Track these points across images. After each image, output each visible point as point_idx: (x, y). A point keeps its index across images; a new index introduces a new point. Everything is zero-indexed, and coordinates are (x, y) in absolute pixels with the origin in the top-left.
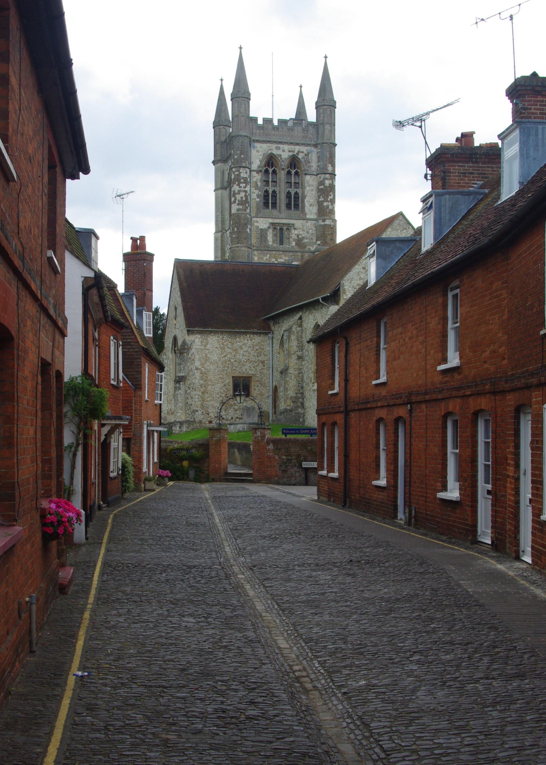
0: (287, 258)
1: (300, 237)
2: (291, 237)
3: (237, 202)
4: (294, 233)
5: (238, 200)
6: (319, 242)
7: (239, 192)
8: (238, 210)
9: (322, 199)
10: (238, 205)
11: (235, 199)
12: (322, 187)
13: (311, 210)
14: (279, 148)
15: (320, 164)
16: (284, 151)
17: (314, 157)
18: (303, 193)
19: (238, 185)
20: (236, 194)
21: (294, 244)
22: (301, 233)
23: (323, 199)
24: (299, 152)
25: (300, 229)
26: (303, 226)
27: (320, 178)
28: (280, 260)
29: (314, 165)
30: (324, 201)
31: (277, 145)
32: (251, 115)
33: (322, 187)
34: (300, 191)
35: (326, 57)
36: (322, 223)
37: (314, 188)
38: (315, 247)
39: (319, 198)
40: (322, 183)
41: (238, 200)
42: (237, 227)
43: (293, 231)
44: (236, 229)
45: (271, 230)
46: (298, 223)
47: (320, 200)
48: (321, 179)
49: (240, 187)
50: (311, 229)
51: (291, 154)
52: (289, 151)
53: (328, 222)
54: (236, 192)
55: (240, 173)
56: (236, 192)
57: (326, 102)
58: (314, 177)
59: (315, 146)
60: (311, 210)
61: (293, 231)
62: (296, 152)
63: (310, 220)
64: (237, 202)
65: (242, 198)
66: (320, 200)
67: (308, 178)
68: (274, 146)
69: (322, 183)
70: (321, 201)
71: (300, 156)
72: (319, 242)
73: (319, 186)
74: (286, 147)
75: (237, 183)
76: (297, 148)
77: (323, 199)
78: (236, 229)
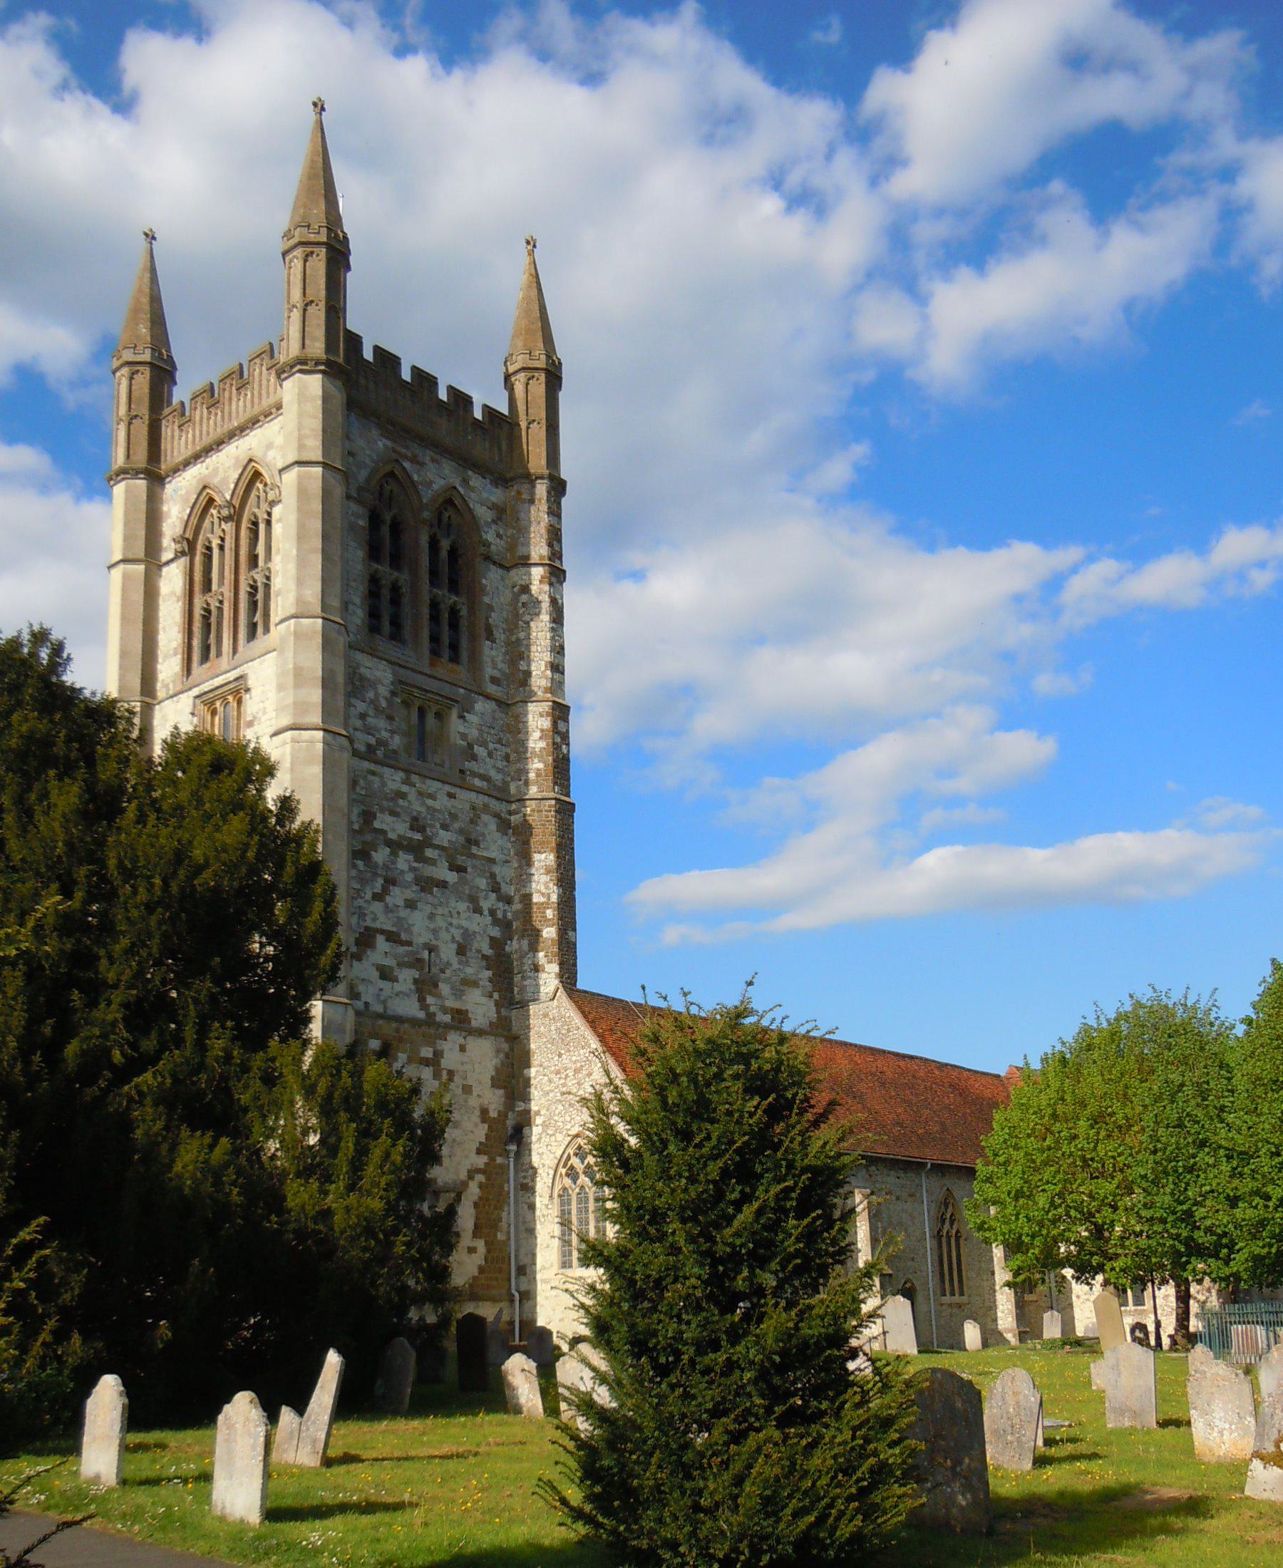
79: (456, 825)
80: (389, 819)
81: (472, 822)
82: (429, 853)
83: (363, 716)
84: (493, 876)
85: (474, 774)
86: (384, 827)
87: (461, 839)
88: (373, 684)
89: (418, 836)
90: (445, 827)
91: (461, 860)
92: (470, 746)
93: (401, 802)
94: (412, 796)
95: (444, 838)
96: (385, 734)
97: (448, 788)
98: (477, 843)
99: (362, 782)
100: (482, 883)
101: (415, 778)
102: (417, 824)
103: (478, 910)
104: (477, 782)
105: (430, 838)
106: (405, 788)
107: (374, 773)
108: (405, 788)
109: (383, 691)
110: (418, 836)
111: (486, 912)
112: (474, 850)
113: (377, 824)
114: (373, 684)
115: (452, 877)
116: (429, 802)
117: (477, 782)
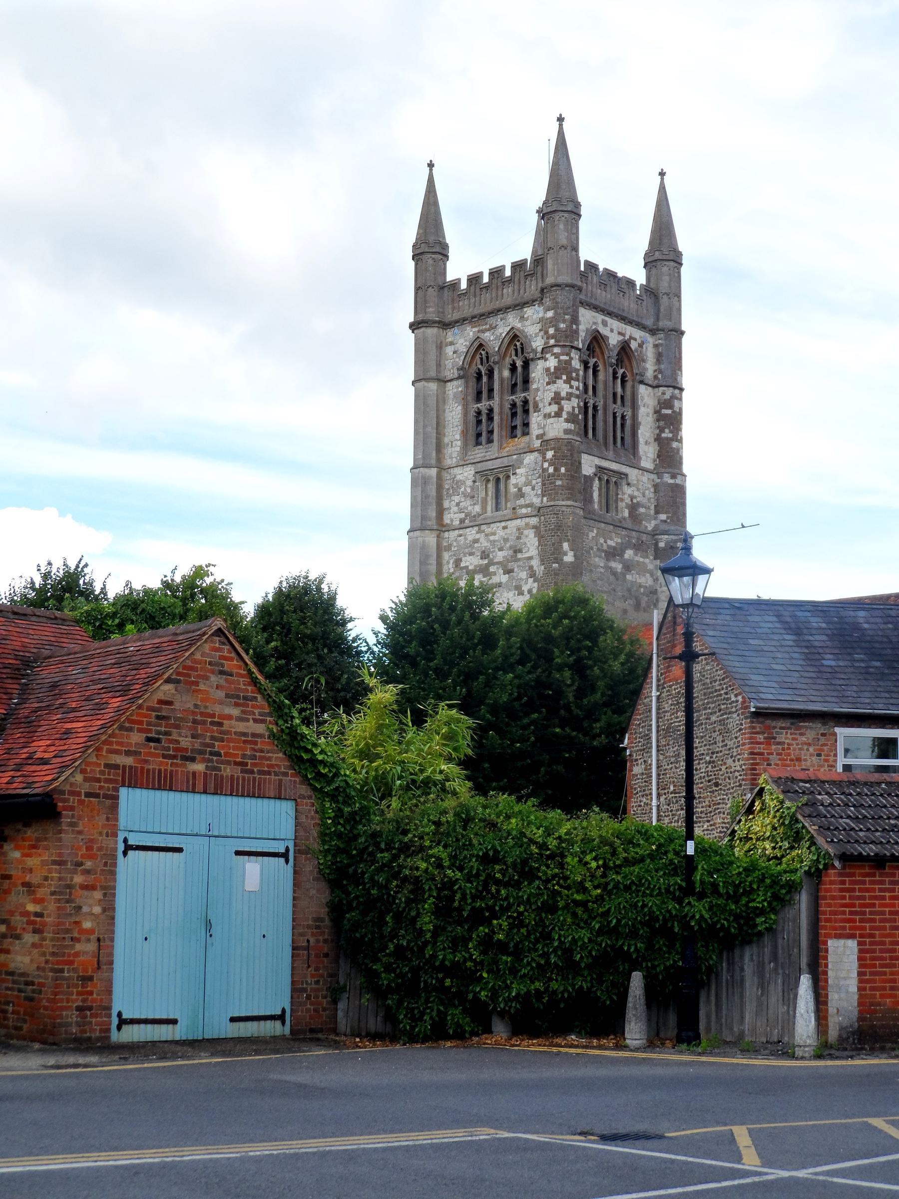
0: (619, 540)
1: (635, 501)
2: (622, 500)
3: (565, 415)
4: (627, 491)
5: (568, 413)
6: (663, 517)
7: (569, 396)
8: (567, 431)
9: (667, 434)
10: (567, 421)
11: (561, 409)
12: (669, 412)
13: (648, 452)
14: (605, 324)
15: (662, 367)
16: (612, 331)
17: (650, 353)
18: (634, 417)
19: (567, 382)
20: (563, 399)
21: (626, 513)
22: (636, 493)
23: (670, 435)
24: (631, 338)
25: (634, 485)
26: (638, 481)
27: (664, 393)
28: (610, 543)
29: (650, 368)
30: (672, 439)
31: (603, 317)
32: (586, 253)
33: (669, 412)
34: (629, 414)
35: (662, 174)
36: (671, 481)
37: (650, 411)
38: (653, 523)
39: (662, 430)
40: (668, 404)
41: (568, 413)
42: (565, 465)
43: (625, 488)
44: (563, 470)
45: (596, 482)
46: (633, 473)
47: (663, 435)
48: (667, 396)
49: (571, 387)
50: (648, 489)
51: (621, 338)
52: (620, 333)
53: (678, 481)
54: (563, 394)
55: (571, 359)
56: (563, 394)
57: (663, 252)
58: (650, 389)
59: (653, 332)
60: (648, 452)
61: (625, 488)
62: (627, 337)
63: (647, 471)
64: (565, 415)
65: (573, 408)
66: (663, 435)
67: (642, 389)
68: (600, 317)
69: (668, 404)
70: (667, 438)
71: (634, 345)
72: (663, 517)
73: (661, 408)
74: (614, 324)
75: (564, 377)
76: (630, 331)
77: (670, 435)
78: (563, 470)
79: (508, 545)
80: (468, 558)
81: (519, 538)
82: (492, 569)
83: (458, 504)
84: (531, 568)
85: (521, 507)
86: (468, 564)
87: (511, 552)
88: (463, 483)
89: (486, 561)
90: (501, 549)
91: (510, 566)
92: (520, 490)
93: (476, 545)
94: (481, 536)
95: (500, 556)
96: (470, 508)
97: (503, 524)
98: (520, 551)
99: (455, 544)
100: (524, 575)
101: (484, 527)
102: (485, 555)
103: (521, 593)
104: (524, 511)
105: (492, 560)
106: (478, 536)
107: (460, 536)
108: (478, 536)
109: (469, 483)
110: (486, 561)
111: (526, 593)
112: (519, 556)
113: (463, 564)
114: (463, 483)
115: (504, 578)
116: (492, 538)
117: (524, 511)
